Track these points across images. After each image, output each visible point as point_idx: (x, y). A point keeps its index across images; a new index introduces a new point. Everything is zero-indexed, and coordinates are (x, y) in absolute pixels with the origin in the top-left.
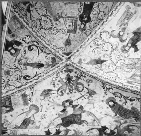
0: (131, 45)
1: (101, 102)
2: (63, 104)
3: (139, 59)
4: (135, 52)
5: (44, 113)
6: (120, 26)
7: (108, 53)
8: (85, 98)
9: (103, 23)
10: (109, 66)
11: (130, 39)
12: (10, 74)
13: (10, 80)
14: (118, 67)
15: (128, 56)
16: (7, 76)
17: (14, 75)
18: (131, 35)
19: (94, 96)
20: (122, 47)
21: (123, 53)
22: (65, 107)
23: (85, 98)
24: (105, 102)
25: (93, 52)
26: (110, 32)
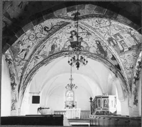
1: (93, 40)
2: (71, 32)
5: (60, 39)
8: (85, 34)
12: (35, 30)
13: (36, 34)
16: (33, 31)
17: (37, 29)
19: (90, 36)
22: (72, 34)
23: (85, 34)
24: (95, 41)
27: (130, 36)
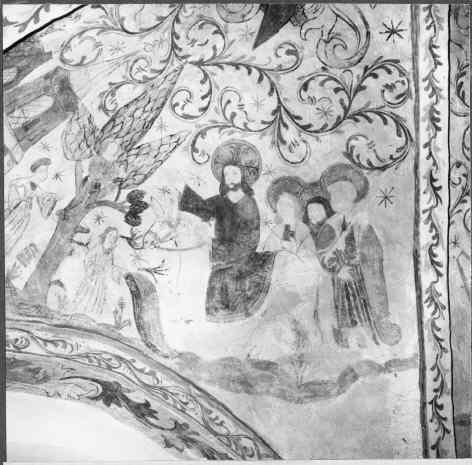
0: (227, 201)
3: (139, 178)
4: (188, 190)
6: (350, 239)
7: (289, 84)
9: (436, 189)
10: (218, 32)
11: (258, 218)
14: (177, 64)
15: (194, 150)
18: (267, 239)
20: (260, 159)
21: (229, 144)
25: (359, 22)
26: (373, 178)
27: (62, 205)
